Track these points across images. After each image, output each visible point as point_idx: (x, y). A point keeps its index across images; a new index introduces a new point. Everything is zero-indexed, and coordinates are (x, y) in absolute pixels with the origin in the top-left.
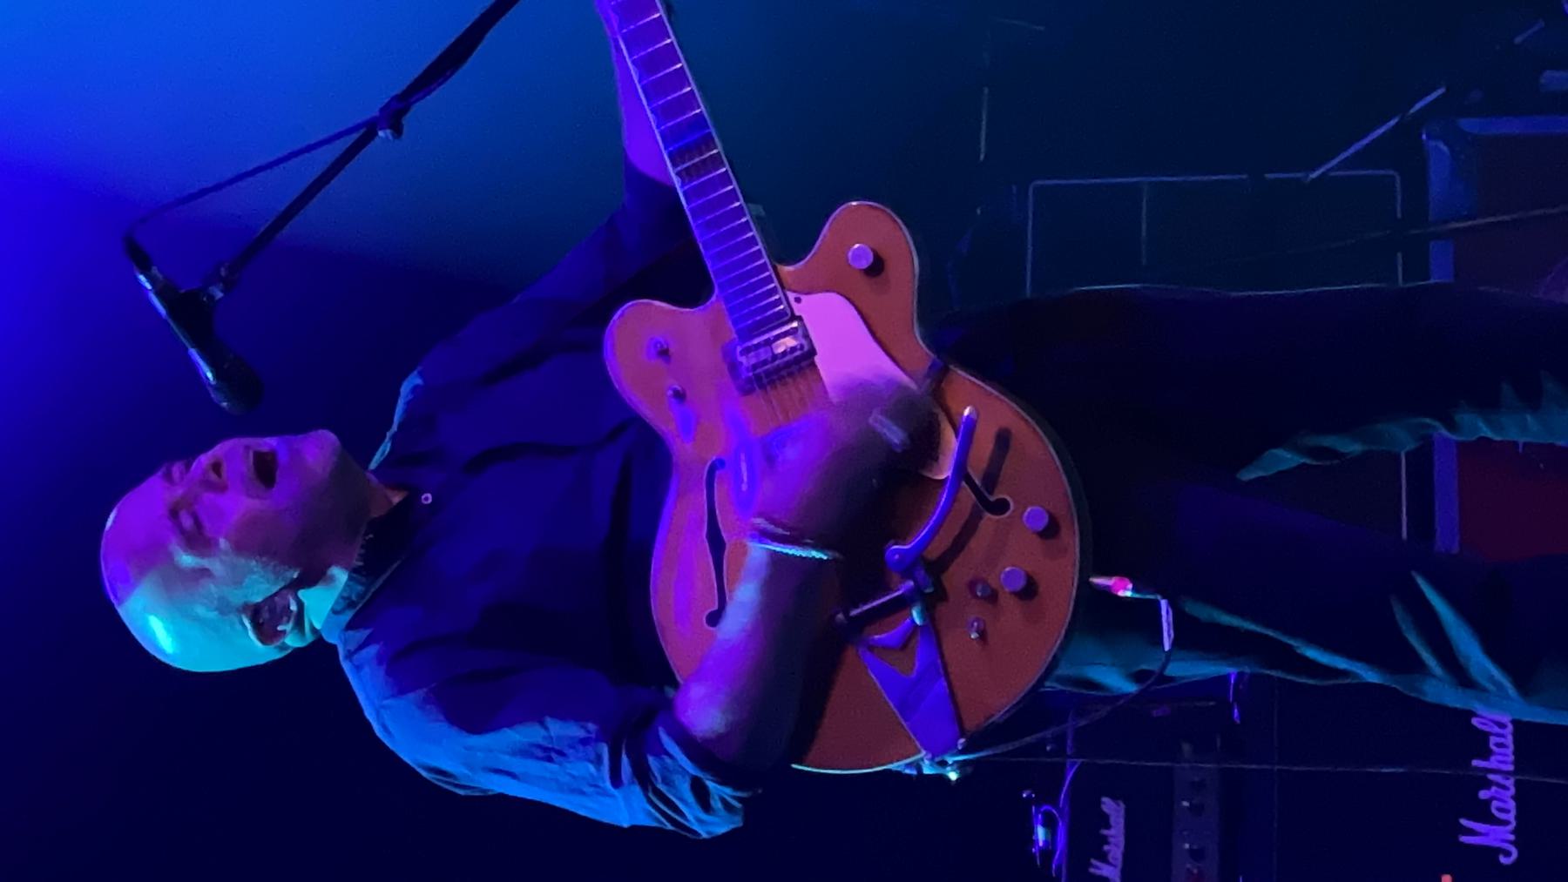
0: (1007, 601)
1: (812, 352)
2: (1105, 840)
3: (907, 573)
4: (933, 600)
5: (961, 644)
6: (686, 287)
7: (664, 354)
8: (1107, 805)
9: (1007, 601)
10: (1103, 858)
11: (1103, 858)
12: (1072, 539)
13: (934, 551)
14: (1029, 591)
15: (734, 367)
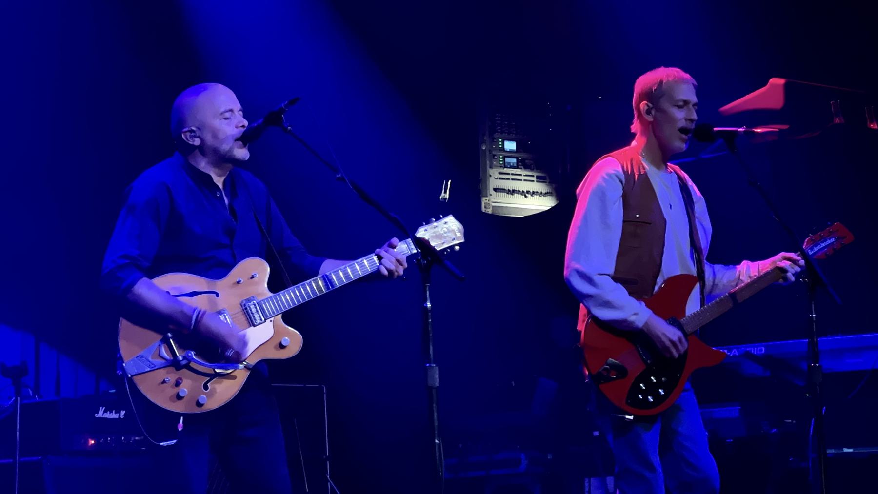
0: (175, 390)
1: (254, 326)
2: (111, 412)
3: (184, 358)
4: (174, 364)
5: (162, 374)
6: (276, 285)
7: (252, 277)
8: (123, 413)
9: (175, 390)
10: (105, 412)
11: (105, 412)
12: (198, 410)
13: (192, 365)
14: (179, 397)
15: (249, 300)
